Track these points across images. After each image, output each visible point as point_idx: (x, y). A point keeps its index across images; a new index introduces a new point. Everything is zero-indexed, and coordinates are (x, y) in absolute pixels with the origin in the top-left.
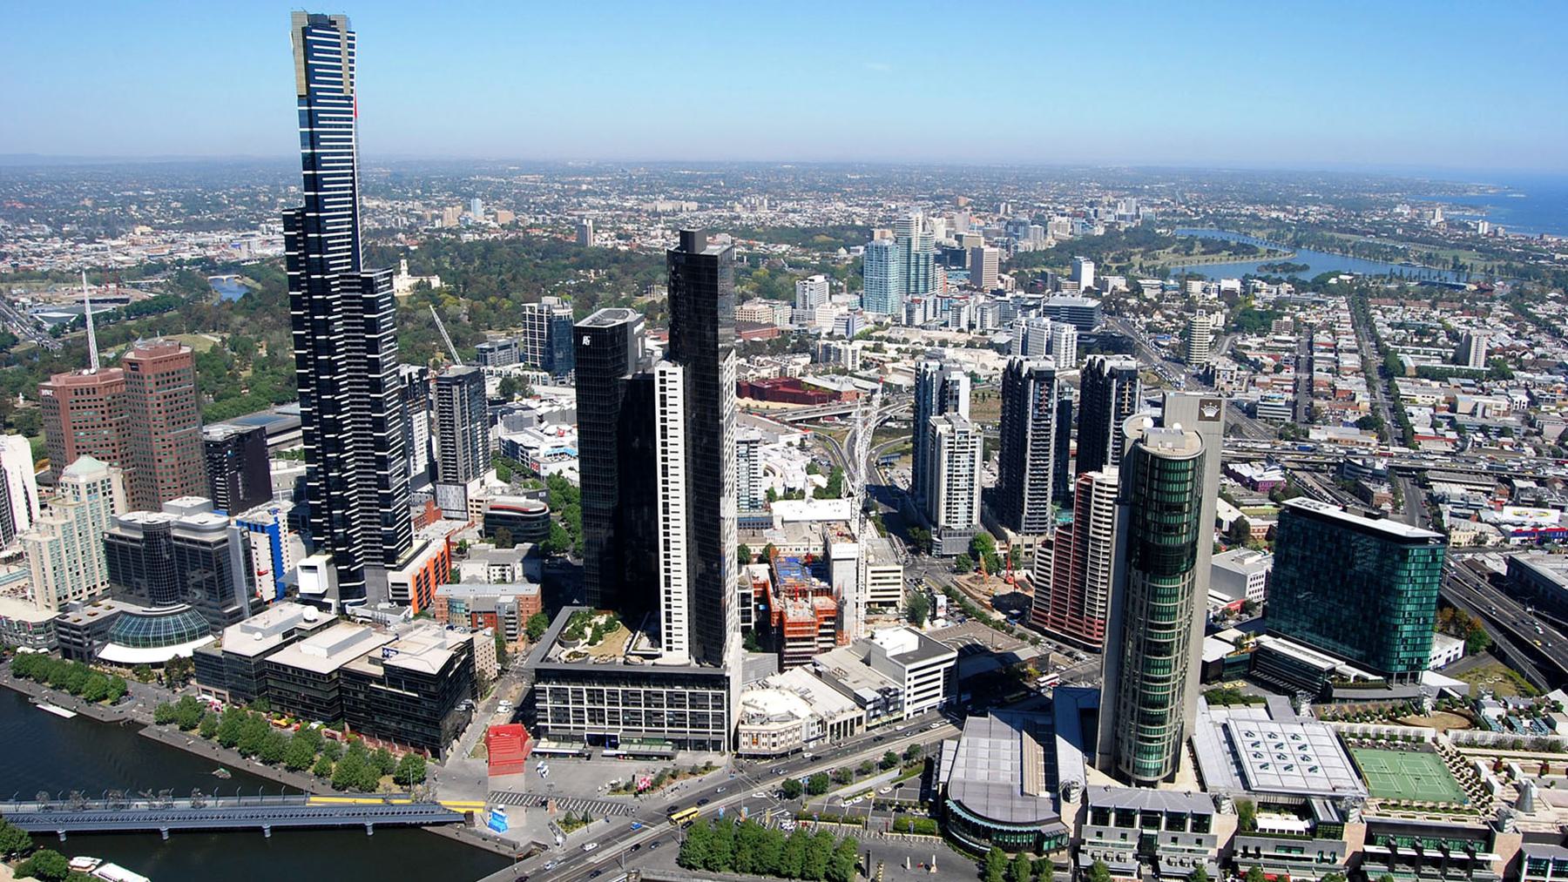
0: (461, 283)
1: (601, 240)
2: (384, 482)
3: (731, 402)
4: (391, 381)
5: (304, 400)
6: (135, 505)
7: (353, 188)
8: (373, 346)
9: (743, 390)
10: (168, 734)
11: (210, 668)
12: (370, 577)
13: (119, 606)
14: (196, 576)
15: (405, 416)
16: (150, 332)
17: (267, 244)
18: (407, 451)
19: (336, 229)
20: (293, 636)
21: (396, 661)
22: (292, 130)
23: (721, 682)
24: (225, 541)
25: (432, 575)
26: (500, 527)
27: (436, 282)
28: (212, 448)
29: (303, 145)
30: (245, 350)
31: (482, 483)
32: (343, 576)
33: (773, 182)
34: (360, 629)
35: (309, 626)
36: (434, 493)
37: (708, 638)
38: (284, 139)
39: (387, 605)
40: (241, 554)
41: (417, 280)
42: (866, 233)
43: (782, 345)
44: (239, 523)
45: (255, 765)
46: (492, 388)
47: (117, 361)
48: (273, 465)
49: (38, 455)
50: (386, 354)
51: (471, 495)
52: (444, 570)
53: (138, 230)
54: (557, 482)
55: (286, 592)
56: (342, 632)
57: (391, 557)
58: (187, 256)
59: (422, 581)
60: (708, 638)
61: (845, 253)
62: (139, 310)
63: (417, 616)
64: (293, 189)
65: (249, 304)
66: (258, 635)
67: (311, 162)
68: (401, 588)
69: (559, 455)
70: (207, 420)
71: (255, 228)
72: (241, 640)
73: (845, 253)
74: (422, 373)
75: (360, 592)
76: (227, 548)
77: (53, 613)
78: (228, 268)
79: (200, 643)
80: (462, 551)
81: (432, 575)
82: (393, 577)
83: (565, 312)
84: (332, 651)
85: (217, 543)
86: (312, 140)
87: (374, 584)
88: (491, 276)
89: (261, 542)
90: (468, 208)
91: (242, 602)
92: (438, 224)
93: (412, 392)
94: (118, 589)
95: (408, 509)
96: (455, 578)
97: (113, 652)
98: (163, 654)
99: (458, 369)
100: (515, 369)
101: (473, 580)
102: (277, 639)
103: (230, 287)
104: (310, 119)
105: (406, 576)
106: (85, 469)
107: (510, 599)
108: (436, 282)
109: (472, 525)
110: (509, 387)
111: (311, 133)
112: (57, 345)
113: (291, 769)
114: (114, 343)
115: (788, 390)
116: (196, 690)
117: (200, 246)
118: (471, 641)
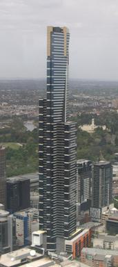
24: (6, 221)
28: (10, 186)
31: (108, 208)
32: (49, 240)
34: (50, 261)
35: (31, 258)
41: (96, 127)
48: (31, 193)
52: (87, 242)
55: (27, 243)
58: (18, 114)
59: (79, 246)
63: (74, 259)
66: (12, 259)
68: (69, 247)
76: (7, 224)
82: (67, 242)
85: (3, 222)
91: (10, 246)
92: (110, 105)
101: (98, 247)
107: (109, 256)
117: (23, 110)
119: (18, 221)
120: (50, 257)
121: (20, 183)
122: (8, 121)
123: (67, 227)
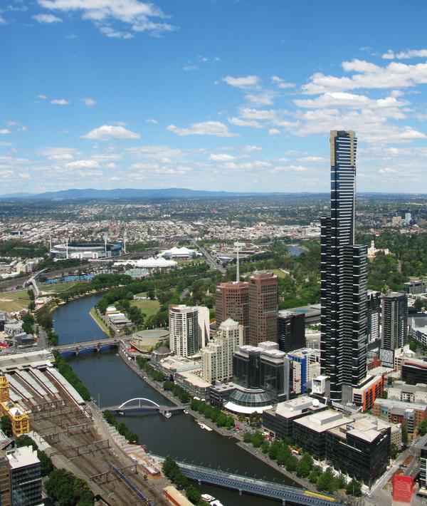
0: (398, 252)
2: (355, 345)
4: (363, 298)
5: (323, 303)
6: (247, 342)
7: (352, 207)
8: (356, 280)
10: (248, 447)
11: (269, 420)
13: (236, 386)
14: (268, 377)
15: (368, 315)
16: (261, 268)
17: (314, 231)
18: (368, 331)
20: (307, 412)
21: (352, 432)
24: (283, 363)
25: (374, 392)
27: (387, 252)
28: (282, 321)
29: (332, 188)
30: (300, 280)
31: (402, 351)
32: (333, 387)
34: (337, 414)
35: (314, 409)
36: (378, 353)
38: (324, 186)
39: (351, 404)
40: (288, 370)
41: (378, 250)
44: (289, 356)
45: (283, 470)
46: (410, 303)
47: (247, 279)
48: (306, 332)
49: (212, 316)
50: (362, 285)
51: (397, 356)
52: (379, 391)
53: (260, 224)
55: (306, 391)
56: (329, 414)
57: (355, 381)
58: (279, 236)
59: (369, 395)
62: (258, 258)
63: (364, 412)
64: (325, 207)
65: (303, 258)
66: (292, 409)
67: (335, 195)
68: (358, 397)
70: (281, 308)
71: (309, 224)
72: (285, 410)
74: (378, 295)
75: (339, 396)
76: (283, 367)
77: (209, 385)
78: (295, 241)
81: (374, 392)
82: (355, 391)
84: (324, 422)
85: (279, 364)
87: (346, 393)
89: (297, 365)
90: (404, 217)
91: (286, 393)
92: (389, 224)
93: (373, 304)
94: (235, 378)
95: (365, 359)
96: (384, 396)
97: (230, 406)
98: (250, 410)
99: (394, 294)
101: (394, 398)
102: (299, 412)
103: (295, 250)
105: (360, 391)
106: (229, 324)
107: (411, 411)
108: (387, 252)
109: (395, 371)
111: (336, 182)
112: (224, 271)
113: (298, 476)
114: (246, 271)
117: (285, 231)
118: (389, 429)
119: (295, 363)
120: (333, 408)
121: (293, 319)
122: (267, 245)
123: (356, 373)
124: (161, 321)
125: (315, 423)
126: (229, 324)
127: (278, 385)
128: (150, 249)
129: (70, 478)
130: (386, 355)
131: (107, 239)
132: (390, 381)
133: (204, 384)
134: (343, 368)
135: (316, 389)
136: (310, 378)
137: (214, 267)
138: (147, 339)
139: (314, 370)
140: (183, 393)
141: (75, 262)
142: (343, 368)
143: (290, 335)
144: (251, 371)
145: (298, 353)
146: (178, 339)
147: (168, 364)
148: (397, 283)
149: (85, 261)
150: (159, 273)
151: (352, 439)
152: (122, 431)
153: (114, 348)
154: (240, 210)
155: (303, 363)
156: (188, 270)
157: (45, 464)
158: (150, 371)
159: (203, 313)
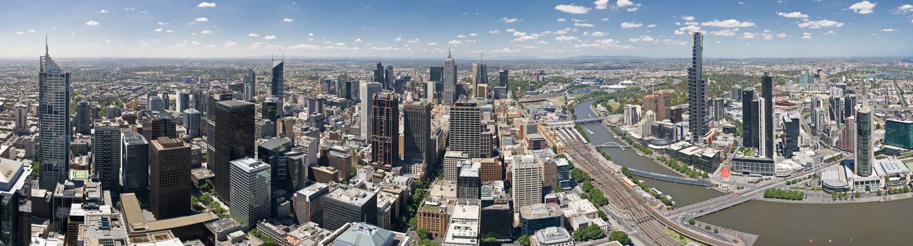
0: (719, 82)
1: (747, 74)
3: (774, 106)
6: (657, 120)
9: (777, 104)
10: (659, 162)
11: (668, 151)
12: (700, 138)
17: (685, 74)
19: (698, 71)
20: (684, 147)
22: (692, 53)
23: (773, 162)
26: (726, 130)
33: (780, 62)
37: (769, 153)
42: (800, 72)
43: (784, 94)
46: (725, 102)
52: (714, 138)
54: (737, 121)
55: (683, 139)
56: (693, 148)
59: (710, 140)
60: (769, 153)
61: (794, 76)
62: (661, 85)
67: (694, 59)
69: (738, 116)
72: (675, 147)
73: (794, 76)
79: (667, 147)
80: (718, 134)
83: (739, 87)
86: (694, 55)
88: (726, 80)
89: (679, 129)
93: (710, 103)
97: (650, 146)
98: (659, 147)
100: (729, 99)
103: (676, 82)
104: (694, 51)
106: (650, 112)
110: (728, 102)
115: (785, 103)
116: (666, 156)
124: (620, 111)
125: (687, 151)
126: (650, 112)
127: (671, 137)
128: (616, 81)
129: (581, 172)
130: (716, 123)
131: (597, 77)
132: (718, 134)
133: (639, 137)
134: (699, 129)
135: (687, 138)
136: (684, 134)
137: (642, 89)
138: (614, 119)
139: (686, 131)
140: (630, 140)
141: (584, 86)
142: (699, 129)
143: (675, 116)
144: (660, 131)
145: (679, 124)
146: (628, 118)
147: (623, 129)
148: (718, 94)
149: (588, 85)
150: (619, 91)
151: (704, 157)
152: (604, 155)
153: (601, 121)
154: (653, 65)
155: (682, 127)
156: (631, 90)
157: (571, 166)
158: (616, 131)
159: (639, 108)
